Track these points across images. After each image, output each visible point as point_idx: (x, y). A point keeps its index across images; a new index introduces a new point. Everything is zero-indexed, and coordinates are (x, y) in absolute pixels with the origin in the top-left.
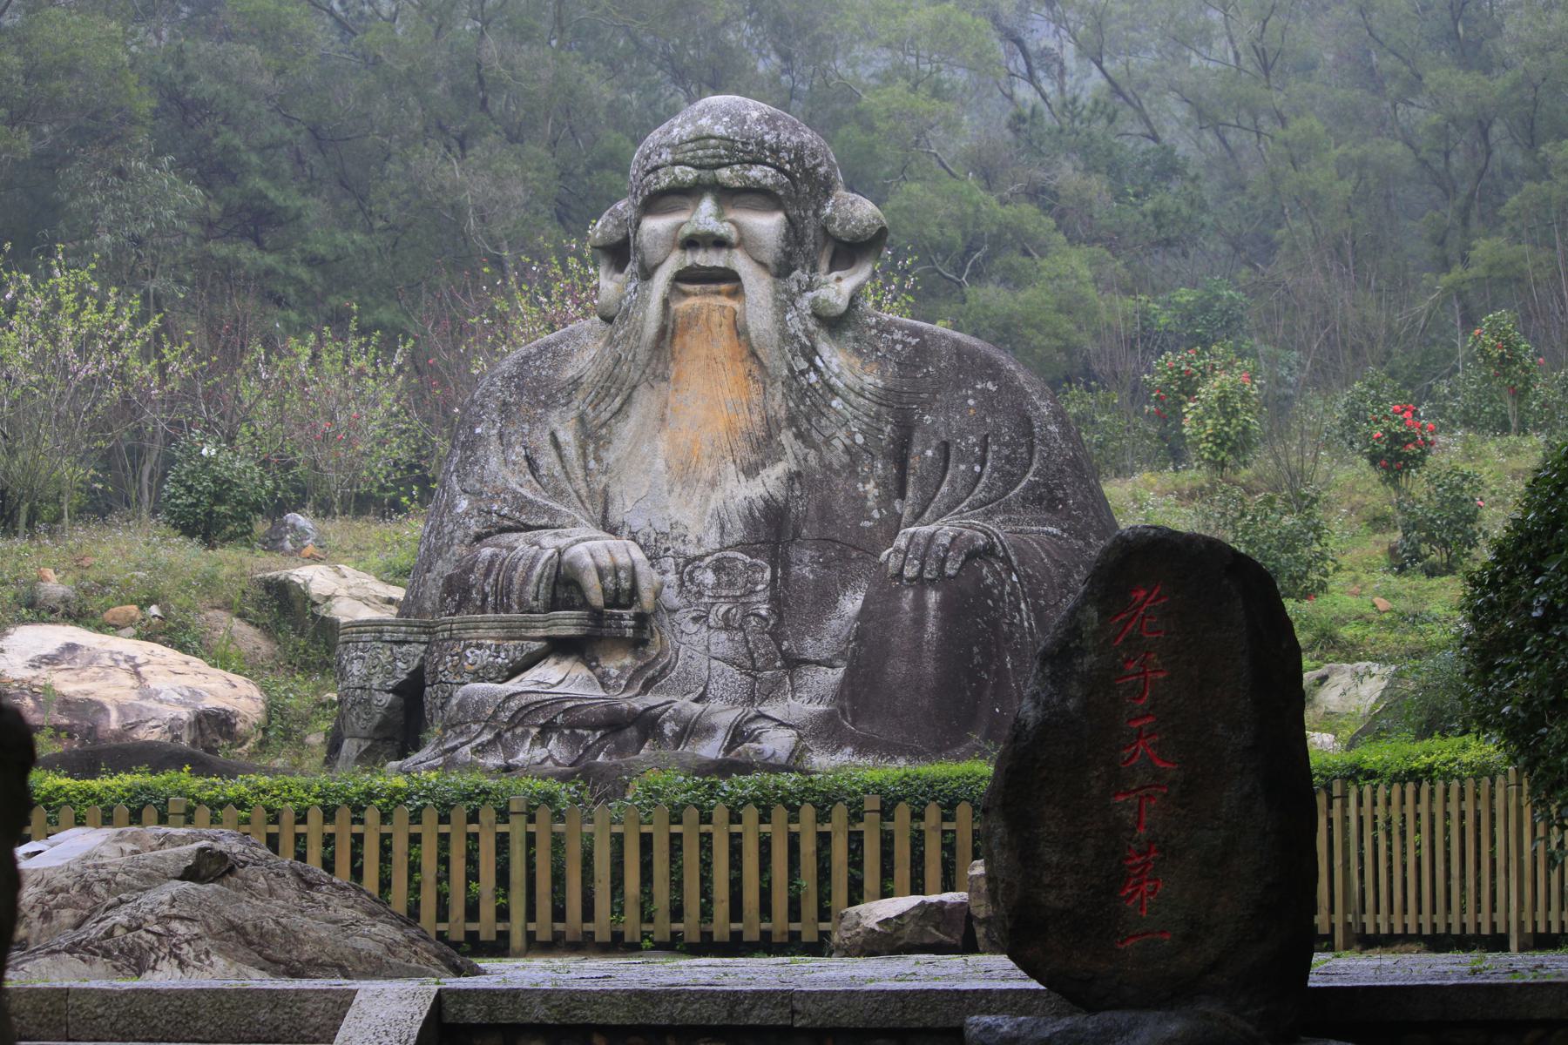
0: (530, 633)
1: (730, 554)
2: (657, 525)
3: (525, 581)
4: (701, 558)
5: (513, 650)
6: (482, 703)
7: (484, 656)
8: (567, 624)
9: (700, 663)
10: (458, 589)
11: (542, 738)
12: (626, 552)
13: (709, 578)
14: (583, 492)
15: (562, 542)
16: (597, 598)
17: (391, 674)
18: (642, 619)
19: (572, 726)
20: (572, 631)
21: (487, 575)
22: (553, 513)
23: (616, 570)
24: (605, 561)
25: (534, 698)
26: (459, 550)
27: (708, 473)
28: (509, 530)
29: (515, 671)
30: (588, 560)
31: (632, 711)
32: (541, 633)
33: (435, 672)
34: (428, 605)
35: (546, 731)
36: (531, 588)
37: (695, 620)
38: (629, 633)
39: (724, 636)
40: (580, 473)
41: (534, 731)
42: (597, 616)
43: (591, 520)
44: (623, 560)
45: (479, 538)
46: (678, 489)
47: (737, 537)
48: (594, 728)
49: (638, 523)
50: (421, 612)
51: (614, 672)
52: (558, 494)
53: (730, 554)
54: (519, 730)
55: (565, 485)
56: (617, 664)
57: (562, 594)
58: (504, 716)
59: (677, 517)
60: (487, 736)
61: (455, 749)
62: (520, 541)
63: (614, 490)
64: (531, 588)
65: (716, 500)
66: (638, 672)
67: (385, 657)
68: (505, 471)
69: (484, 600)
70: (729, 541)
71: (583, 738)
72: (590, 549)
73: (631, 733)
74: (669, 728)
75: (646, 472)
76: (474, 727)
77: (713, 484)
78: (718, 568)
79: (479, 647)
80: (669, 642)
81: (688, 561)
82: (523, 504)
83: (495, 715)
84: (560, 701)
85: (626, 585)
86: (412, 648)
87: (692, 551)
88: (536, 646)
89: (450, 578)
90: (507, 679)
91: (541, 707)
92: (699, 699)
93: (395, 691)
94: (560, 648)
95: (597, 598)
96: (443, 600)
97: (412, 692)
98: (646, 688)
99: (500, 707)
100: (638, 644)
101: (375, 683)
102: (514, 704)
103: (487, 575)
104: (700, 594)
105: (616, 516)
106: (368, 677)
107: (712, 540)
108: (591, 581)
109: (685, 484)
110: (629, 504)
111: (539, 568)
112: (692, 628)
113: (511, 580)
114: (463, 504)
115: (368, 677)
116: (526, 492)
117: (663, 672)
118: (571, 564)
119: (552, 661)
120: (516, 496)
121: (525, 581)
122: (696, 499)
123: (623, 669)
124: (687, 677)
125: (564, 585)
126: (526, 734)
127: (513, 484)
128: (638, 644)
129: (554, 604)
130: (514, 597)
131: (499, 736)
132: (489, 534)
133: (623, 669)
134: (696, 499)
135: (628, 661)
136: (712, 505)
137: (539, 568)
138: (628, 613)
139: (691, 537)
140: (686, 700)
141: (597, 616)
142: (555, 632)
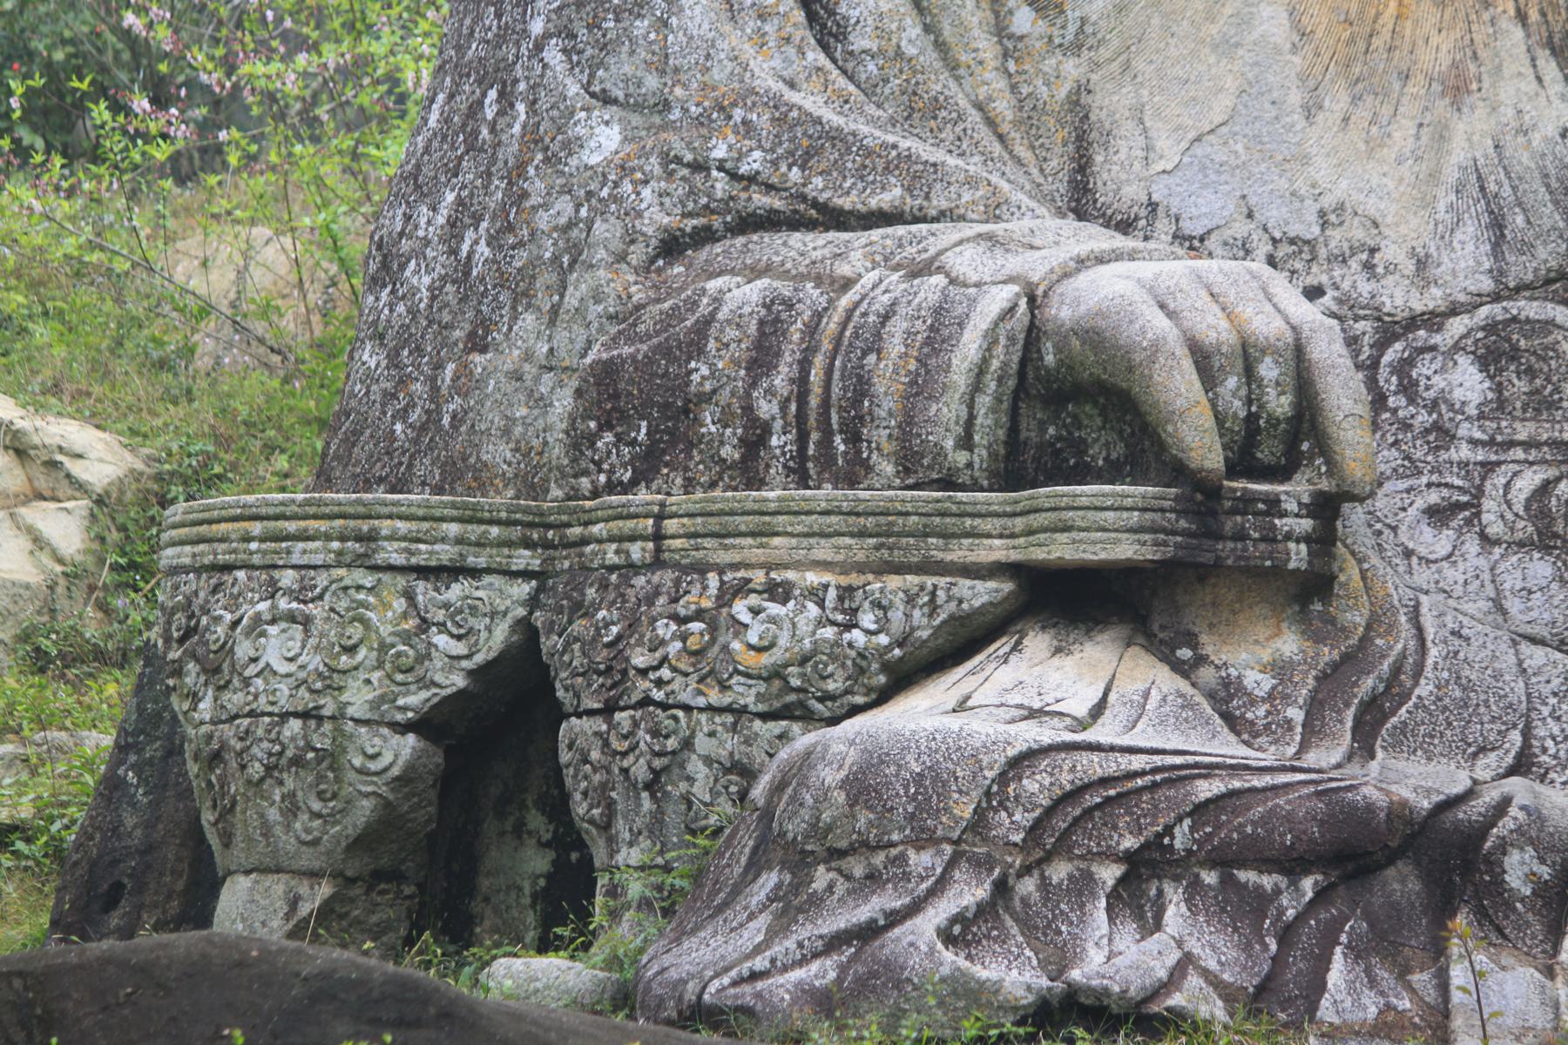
0: (958, 553)
1: (1531, 309)
2: (1275, 215)
3: (922, 386)
4: (1434, 320)
5: (898, 609)
6: (932, 785)
7: (795, 627)
8: (1103, 523)
9: (1488, 652)
10: (643, 407)
11: (1134, 899)
12: (1274, 307)
13: (1467, 383)
14: (1003, 107)
15: (1036, 266)
16: (1204, 449)
17: (413, 670)
18: (1326, 508)
19: (1224, 861)
20: (1126, 550)
21: (761, 360)
22: (919, 176)
23: (1248, 355)
24: (1214, 328)
25: (1095, 766)
26: (608, 282)
27: (1437, 51)
28: (770, 222)
29: (906, 674)
30: (1161, 323)
31: (1399, 812)
32: (996, 551)
33: (616, 672)
34: (498, 453)
35: (1144, 875)
36: (947, 411)
37: (1438, 515)
38: (1298, 556)
39: (1541, 568)
40: (988, 48)
41: (1109, 874)
42: (1202, 498)
43: (1047, 199)
44: (1265, 325)
45: (672, 246)
46: (1337, 101)
47: (1547, 256)
48: (1292, 865)
49: (1203, 207)
50: (458, 473)
51: (1258, 681)
52: (921, 111)
53: (1531, 309)
54: (1060, 871)
55: (939, 83)
56: (1261, 651)
57: (1041, 429)
58: (1012, 824)
59: (1341, 189)
60: (968, 893)
61: (868, 932)
62: (855, 253)
63: (1110, 103)
64: (947, 411)
65: (1469, 138)
66: (1333, 681)
67: (388, 615)
68: (735, 40)
69: (755, 438)
70: (1521, 268)
71: (1261, 902)
72: (1128, 291)
73: (1402, 883)
74: (1520, 870)
75: (1226, 47)
76: (921, 860)
77: (1457, 88)
78: (1494, 353)
79: (779, 592)
80: (1394, 585)
81: (1391, 330)
82: (815, 144)
83: (979, 824)
84: (1179, 776)
85: (1280, 404)
86: (488, 591)
87: (1398, 297)
88: (981, 594)
89: (606, 373)
90: (883, 697)
91: (1115, 796)
92: (1522, 765)
93: (422, 725)
94: (1064, 599)
95: (1204, 449)
96: (579, 442)
97: (498, 733)
98: (1364, 745)
99: (995, 797)
100: (1309, 592)
101: (357, 698)
102: (1035, 786)
103: (761, 360)
104: (1442, 435)
105: (1121, 176)
106: (332, 680)
107: (1465, 264)
108: (1179, 392)
109: (1360, 89)
110: (1169, 150)
111: (969, 346)
112: (1435, 542)
113: (861, 387)
114: (604, 139)
115: (332, 680)
116: (810, 101)
117: (1393, 692)
118: (1093, 336)
119: (1037, 642)
120: (783, 116)
121: (922, 386)
122: (1403, 134)
123: (1281, 669)
124: (1462, 702)
125: (1068, 403)
126: (1083, 885)
127: (765, 74)
128: (1309, 592)
129: (1017, 467)
130: (880, 436)
131: (1002, 888)
132: (704, 236)
133: (1281, 669)
134: (1403, 134)
135: (1289, 644)
136: (1458, 155)
137: (969, 346)
138: (1296, 491)
139: (1392, 252)
140: (1487, 767)
141: (1202, 498)
142: (1061, 550)
